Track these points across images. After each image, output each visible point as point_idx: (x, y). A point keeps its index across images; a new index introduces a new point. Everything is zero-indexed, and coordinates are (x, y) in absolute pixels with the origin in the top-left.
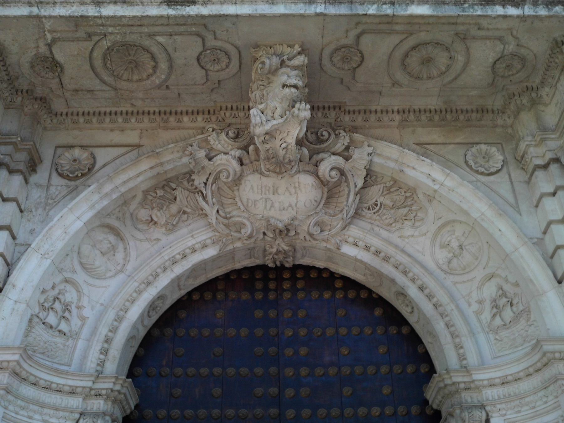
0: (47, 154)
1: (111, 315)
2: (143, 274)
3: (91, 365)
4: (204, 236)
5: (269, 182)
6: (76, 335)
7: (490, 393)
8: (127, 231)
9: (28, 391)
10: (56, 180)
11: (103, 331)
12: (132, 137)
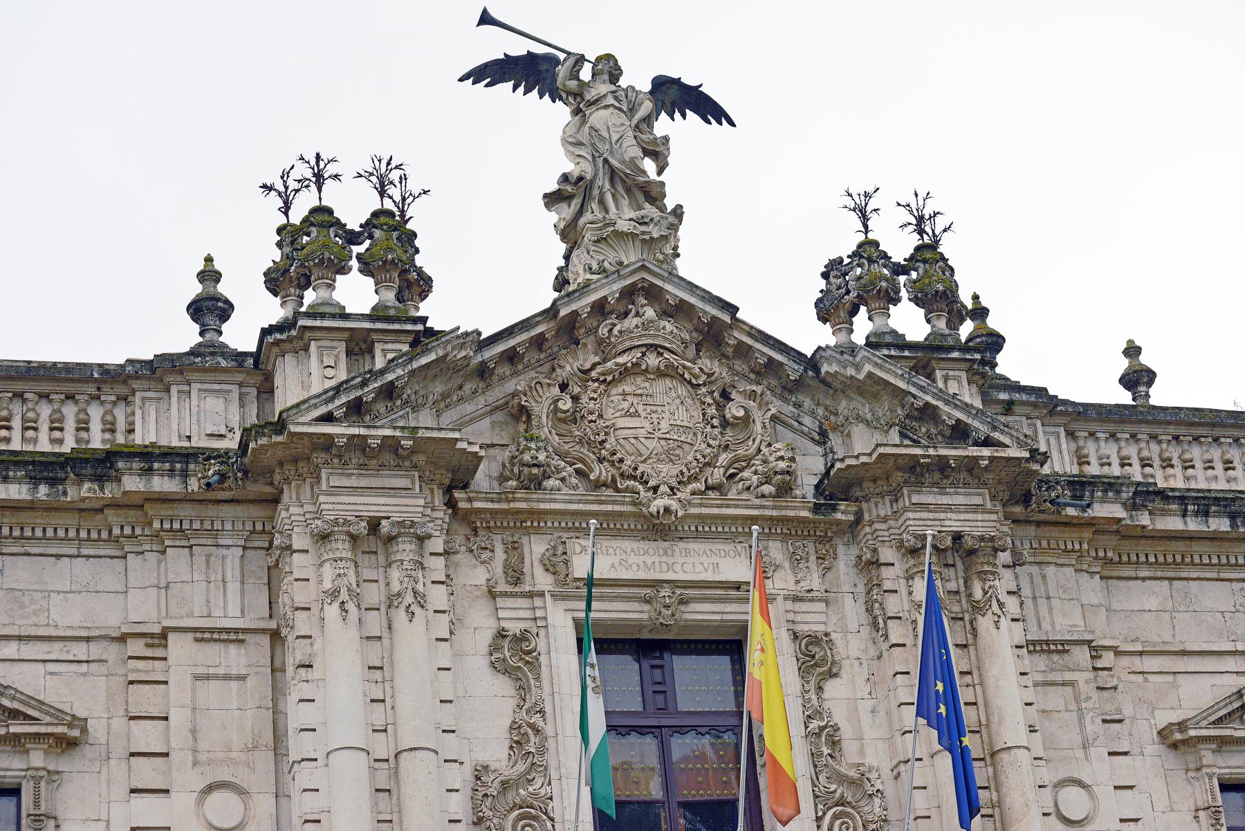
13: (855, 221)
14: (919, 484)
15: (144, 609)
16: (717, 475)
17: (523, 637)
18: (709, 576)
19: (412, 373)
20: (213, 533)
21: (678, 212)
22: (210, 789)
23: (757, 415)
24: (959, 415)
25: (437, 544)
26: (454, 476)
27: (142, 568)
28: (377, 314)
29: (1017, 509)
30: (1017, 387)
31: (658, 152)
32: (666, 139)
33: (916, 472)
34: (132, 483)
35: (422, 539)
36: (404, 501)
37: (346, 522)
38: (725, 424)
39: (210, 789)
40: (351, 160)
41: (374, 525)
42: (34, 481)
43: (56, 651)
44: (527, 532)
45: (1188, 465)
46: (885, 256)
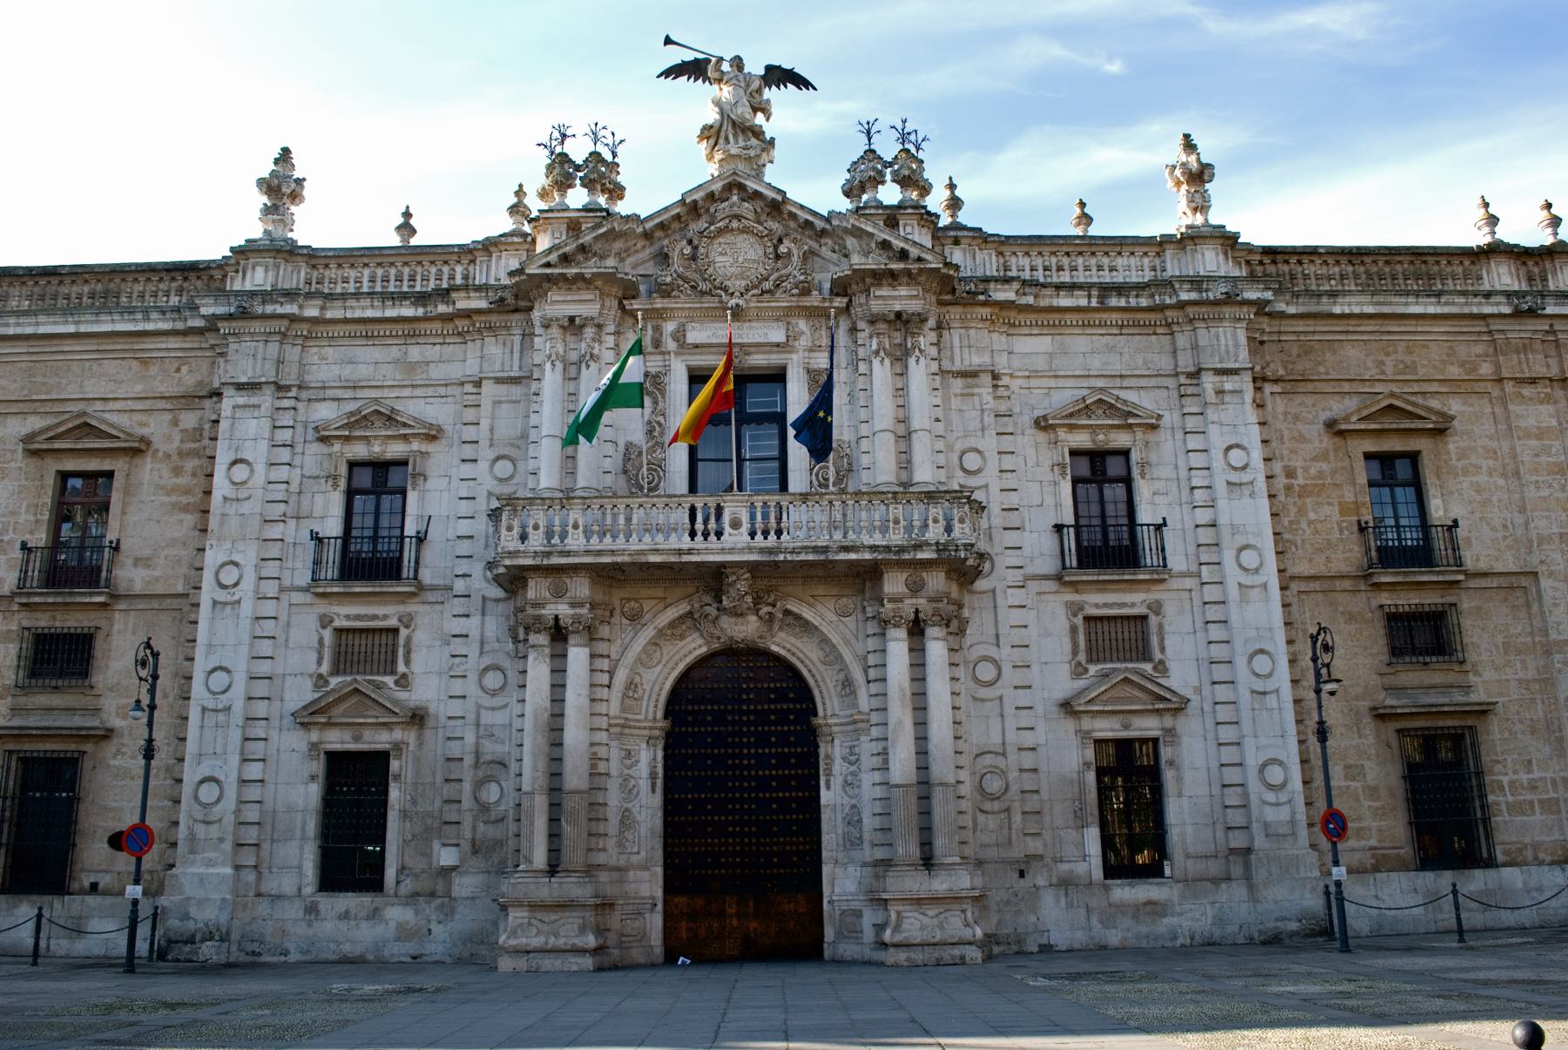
0: (617, 604)
1: (657, 688)
2: (670, 665)
3: (650, 716)
4: (700, 641)
5: (733, 620)
6: (642, 698)
7: (835, 729)
8: (662, 643)
9: (627, 731)
10: (625, 621)
11: (654, 696)
12: (660, 593)
13: (864, 138)
14: (880, 285)
15: (472, 368)
16: (767, 285)
17: (657, 376)
18: (762, 340)
19: (595, 238)
20: (508, 328)
21: (772, 142)
22: (498, 459)
23: (795, 252)
24: (902, 245)
25: (611, 328)
26: (629, 291)
27: (473, 349)
28: (586, 209)
29: (948, 297)
30: (964, 228)
31: (763, 108)
32: (768, 101)
33: (893, 276)
34: (461, 305)
35: (600, 327)
36: (584, 306)
37: (558, 319)
38: (778, 257)
39: (498, 459)
40: (579, 127)
41: (572, 319)
42: (415, 304)
43: (430, 391)
44: (665, 320)
45: (1100, 268)
46: (880, 158)
